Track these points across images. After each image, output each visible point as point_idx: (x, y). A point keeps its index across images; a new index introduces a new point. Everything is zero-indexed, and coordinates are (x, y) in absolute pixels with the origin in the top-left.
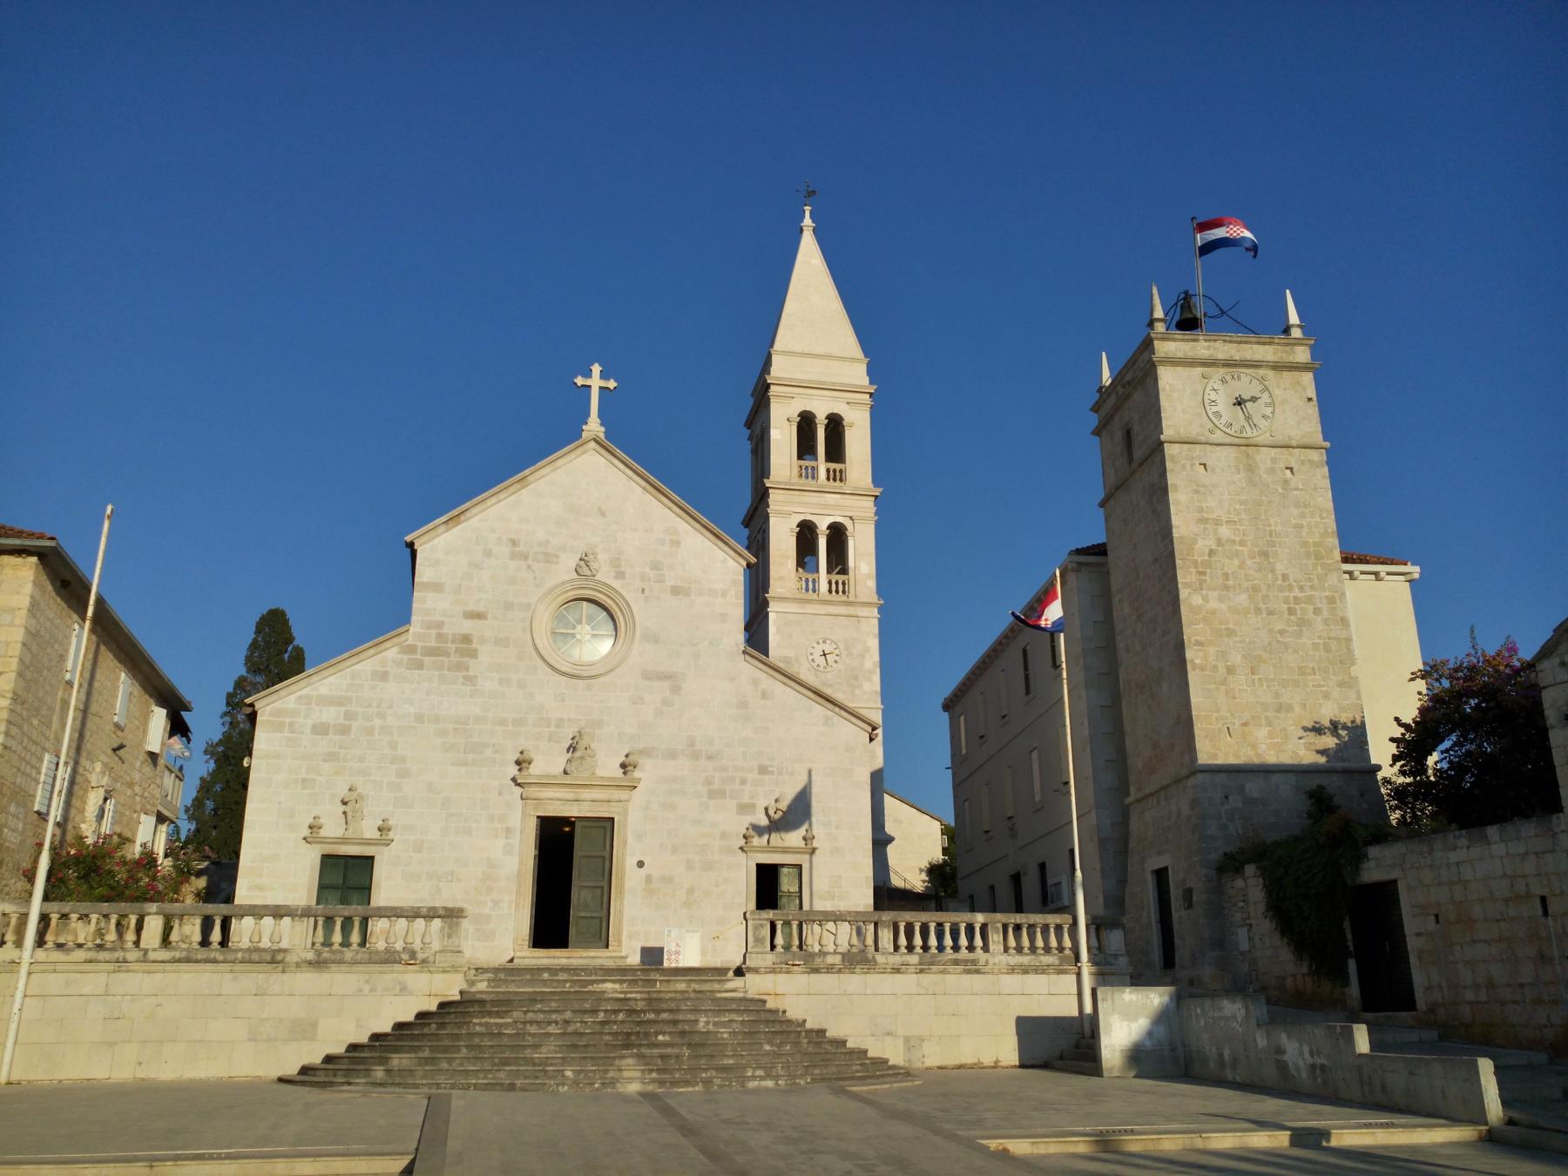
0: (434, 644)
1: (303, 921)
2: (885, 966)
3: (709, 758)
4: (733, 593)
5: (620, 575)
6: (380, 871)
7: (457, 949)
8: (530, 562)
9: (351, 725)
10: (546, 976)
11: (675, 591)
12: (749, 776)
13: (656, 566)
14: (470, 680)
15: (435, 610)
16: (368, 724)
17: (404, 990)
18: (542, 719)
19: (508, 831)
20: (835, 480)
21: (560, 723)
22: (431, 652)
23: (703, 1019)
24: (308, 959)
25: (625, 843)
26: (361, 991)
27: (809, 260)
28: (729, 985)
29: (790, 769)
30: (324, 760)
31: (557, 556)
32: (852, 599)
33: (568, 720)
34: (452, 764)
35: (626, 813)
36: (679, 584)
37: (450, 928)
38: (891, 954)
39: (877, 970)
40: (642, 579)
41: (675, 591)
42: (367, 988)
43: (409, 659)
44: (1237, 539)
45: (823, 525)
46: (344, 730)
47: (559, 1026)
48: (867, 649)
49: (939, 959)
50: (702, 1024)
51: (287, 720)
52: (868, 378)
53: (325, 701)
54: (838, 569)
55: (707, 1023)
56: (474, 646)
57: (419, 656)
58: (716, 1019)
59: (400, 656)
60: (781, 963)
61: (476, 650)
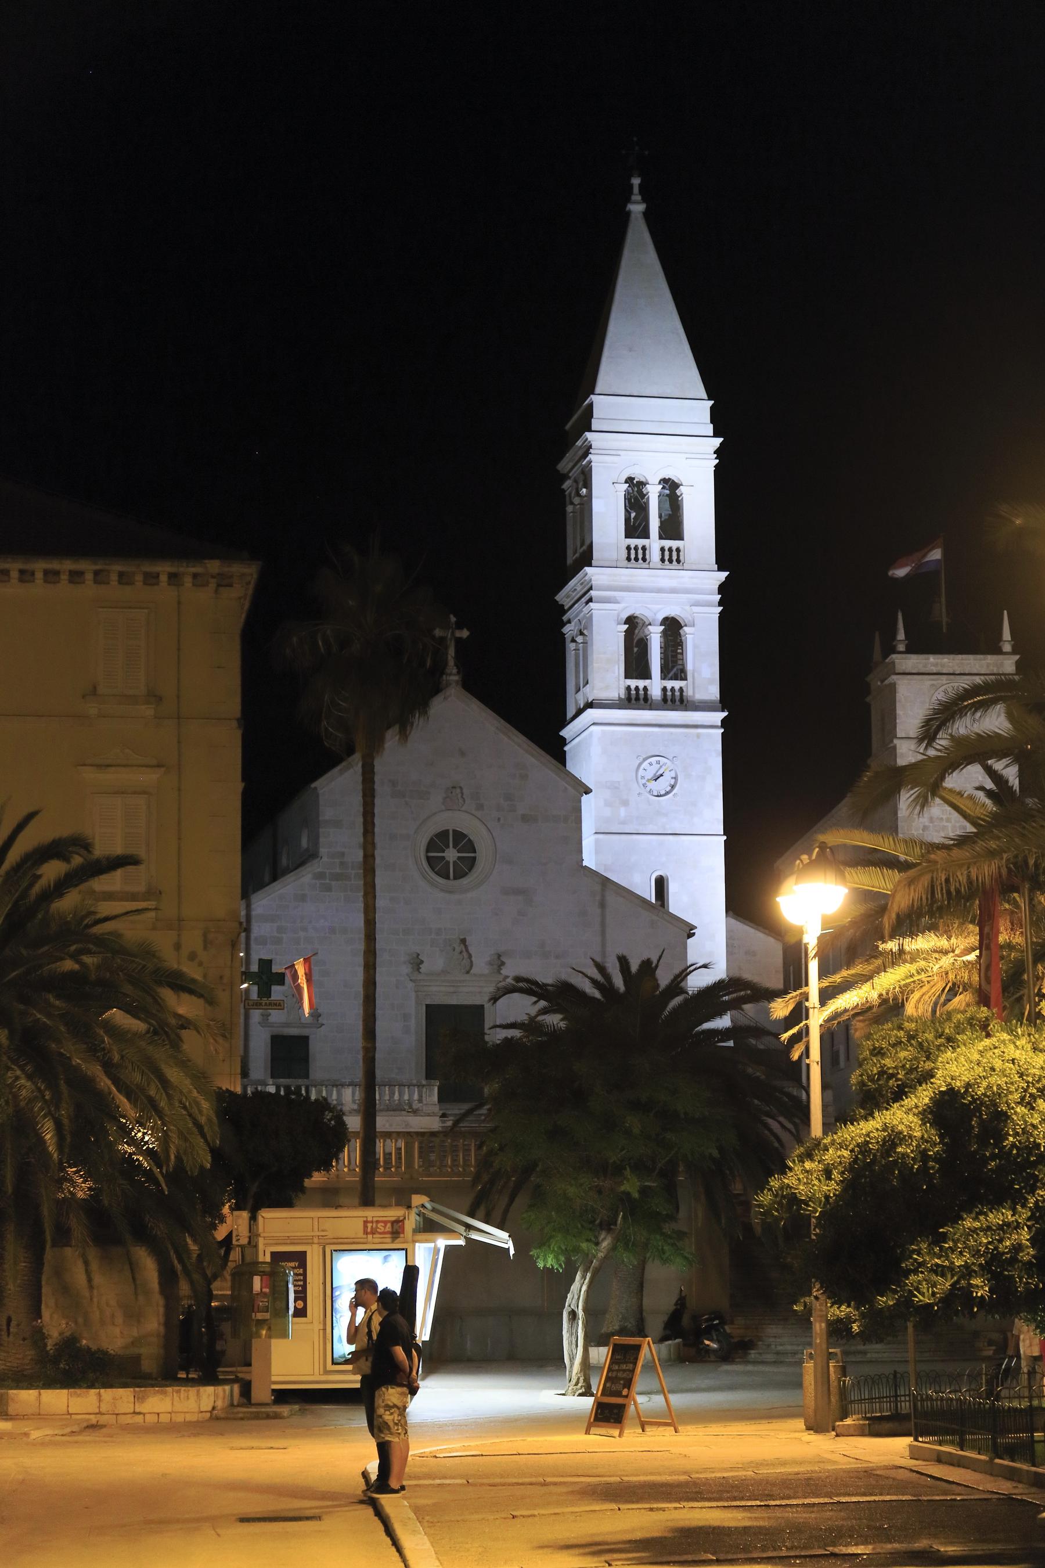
0: (338, 870)
3: (557, 957)
6: (314, 1047)
11: (525, 818)
20: (671, 561)
22: (336, 877)
41: (525, 818)
44: (944, 817)
46: (278, 941)
52: (712, 426)
57: (328, 881)
59: (314, 881)
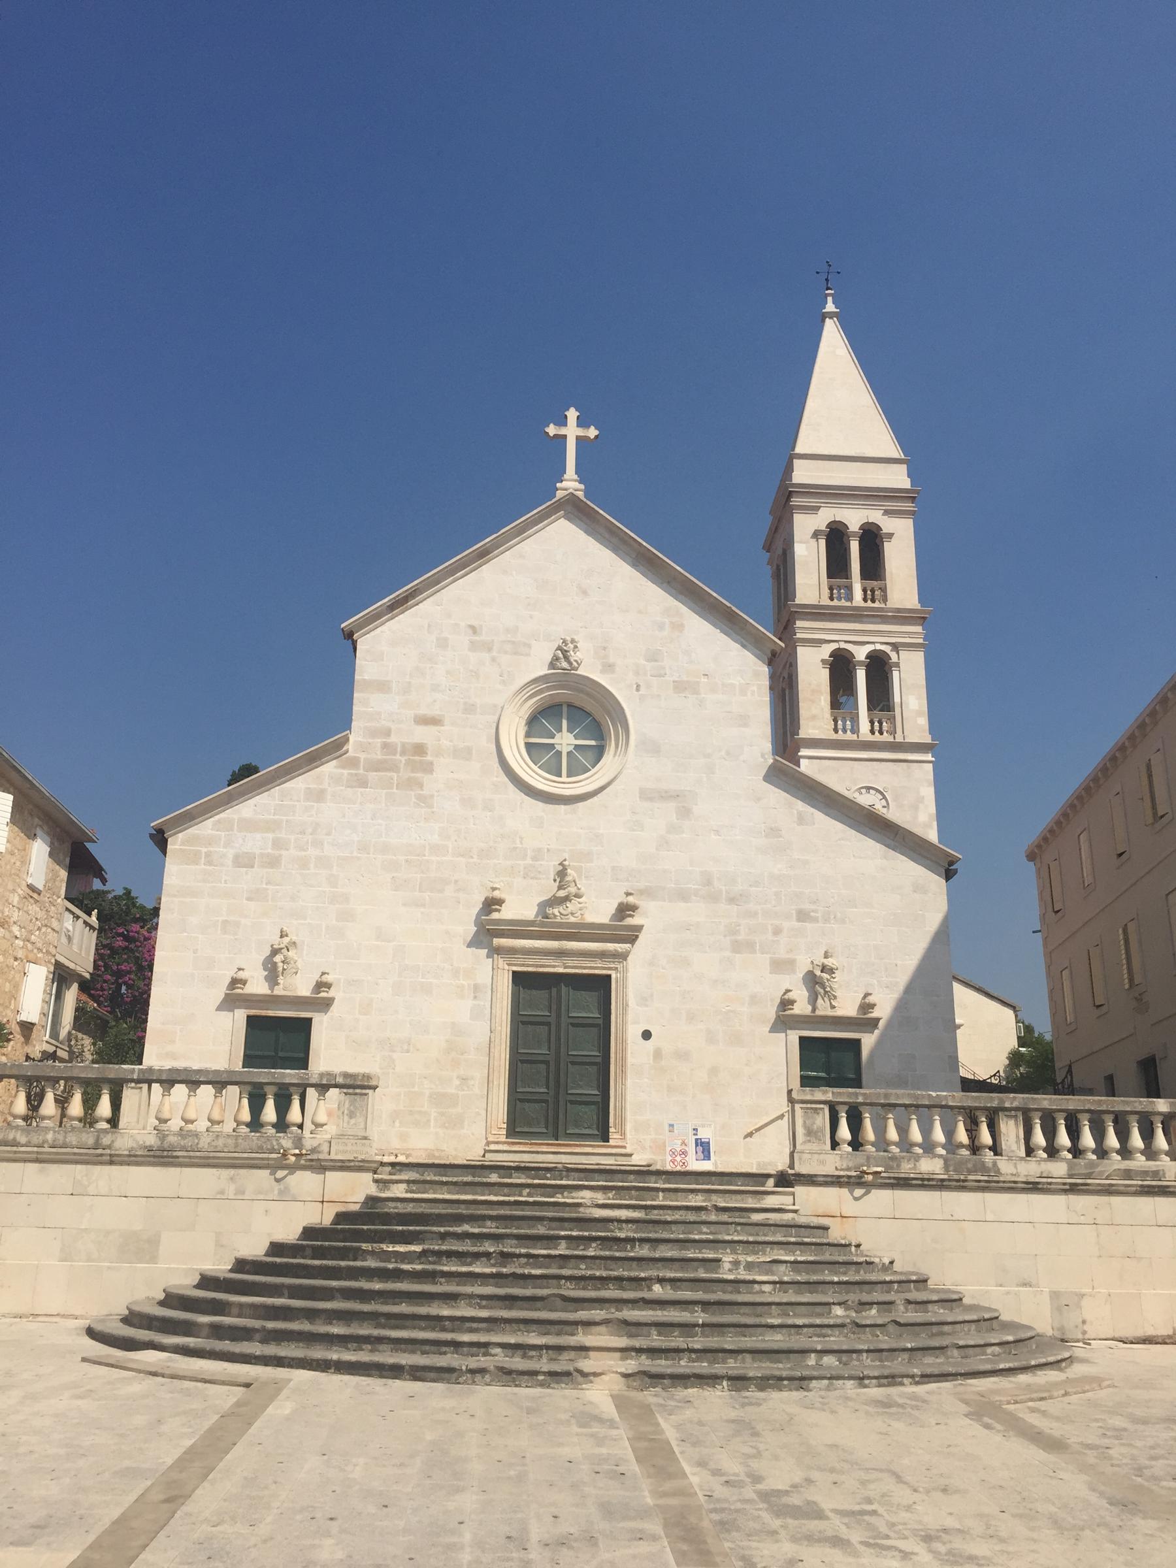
1: (141, 1088)
2: (1013, 1179)
3: (732, 900)
4: (755, 688)
5: (609, 668)
7: (363, 1134)
8: (494, 654)
9: (280, 856)
10: (494, 1178)
11: (680, 687)
12: (786, 925)
13: (653, 657)
14: (424, 800)
15: (379, 713)
16: (303, 853)
17: (285, 1197)
18: (515, 848)
19: (476, 988)
21: (538, 854)
22: (378, 767)
23: (727, 1259)
24: (148, 1144)
25: (625, 1006)
26: (222, 1192)
27: (832, 337)
28: (771, 1201)
29: (839, 915)
30: (248, 899)
31: (529, 646)
32: (899, 739)
33: (548, 850)
34: (404, 905)
35: (625, 970)
36: (685, 679)
37: (352, 1103)
38: (1022, 1159)
39: (1001, 1185)
40: (637, 673)
41: (680, 687)
42: (231, 1191)
43: (351, 774)
45: (861, 653)
46: (273, 862)
47: (492, 1261)
48: (921, 799)
49: (1099, 1169)
50: (727, 1266)
51: (204, 850)
53: (249, 826)
54: (881, 705)
55: (736, 1263)
56: (429, 758)
57: (361, 771)
58: (750, 1259)
60: (848, 1169)
61: (432, 763)
